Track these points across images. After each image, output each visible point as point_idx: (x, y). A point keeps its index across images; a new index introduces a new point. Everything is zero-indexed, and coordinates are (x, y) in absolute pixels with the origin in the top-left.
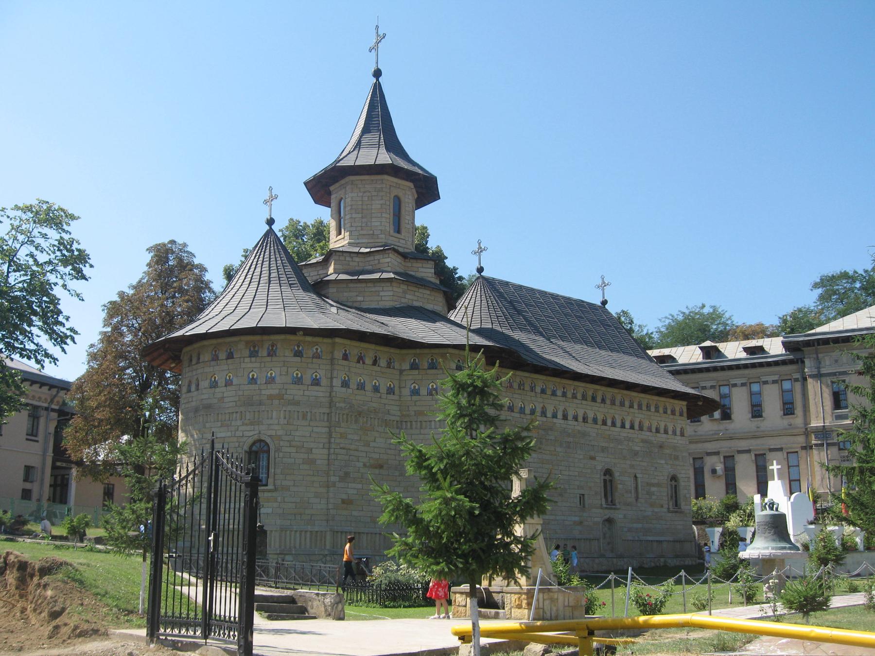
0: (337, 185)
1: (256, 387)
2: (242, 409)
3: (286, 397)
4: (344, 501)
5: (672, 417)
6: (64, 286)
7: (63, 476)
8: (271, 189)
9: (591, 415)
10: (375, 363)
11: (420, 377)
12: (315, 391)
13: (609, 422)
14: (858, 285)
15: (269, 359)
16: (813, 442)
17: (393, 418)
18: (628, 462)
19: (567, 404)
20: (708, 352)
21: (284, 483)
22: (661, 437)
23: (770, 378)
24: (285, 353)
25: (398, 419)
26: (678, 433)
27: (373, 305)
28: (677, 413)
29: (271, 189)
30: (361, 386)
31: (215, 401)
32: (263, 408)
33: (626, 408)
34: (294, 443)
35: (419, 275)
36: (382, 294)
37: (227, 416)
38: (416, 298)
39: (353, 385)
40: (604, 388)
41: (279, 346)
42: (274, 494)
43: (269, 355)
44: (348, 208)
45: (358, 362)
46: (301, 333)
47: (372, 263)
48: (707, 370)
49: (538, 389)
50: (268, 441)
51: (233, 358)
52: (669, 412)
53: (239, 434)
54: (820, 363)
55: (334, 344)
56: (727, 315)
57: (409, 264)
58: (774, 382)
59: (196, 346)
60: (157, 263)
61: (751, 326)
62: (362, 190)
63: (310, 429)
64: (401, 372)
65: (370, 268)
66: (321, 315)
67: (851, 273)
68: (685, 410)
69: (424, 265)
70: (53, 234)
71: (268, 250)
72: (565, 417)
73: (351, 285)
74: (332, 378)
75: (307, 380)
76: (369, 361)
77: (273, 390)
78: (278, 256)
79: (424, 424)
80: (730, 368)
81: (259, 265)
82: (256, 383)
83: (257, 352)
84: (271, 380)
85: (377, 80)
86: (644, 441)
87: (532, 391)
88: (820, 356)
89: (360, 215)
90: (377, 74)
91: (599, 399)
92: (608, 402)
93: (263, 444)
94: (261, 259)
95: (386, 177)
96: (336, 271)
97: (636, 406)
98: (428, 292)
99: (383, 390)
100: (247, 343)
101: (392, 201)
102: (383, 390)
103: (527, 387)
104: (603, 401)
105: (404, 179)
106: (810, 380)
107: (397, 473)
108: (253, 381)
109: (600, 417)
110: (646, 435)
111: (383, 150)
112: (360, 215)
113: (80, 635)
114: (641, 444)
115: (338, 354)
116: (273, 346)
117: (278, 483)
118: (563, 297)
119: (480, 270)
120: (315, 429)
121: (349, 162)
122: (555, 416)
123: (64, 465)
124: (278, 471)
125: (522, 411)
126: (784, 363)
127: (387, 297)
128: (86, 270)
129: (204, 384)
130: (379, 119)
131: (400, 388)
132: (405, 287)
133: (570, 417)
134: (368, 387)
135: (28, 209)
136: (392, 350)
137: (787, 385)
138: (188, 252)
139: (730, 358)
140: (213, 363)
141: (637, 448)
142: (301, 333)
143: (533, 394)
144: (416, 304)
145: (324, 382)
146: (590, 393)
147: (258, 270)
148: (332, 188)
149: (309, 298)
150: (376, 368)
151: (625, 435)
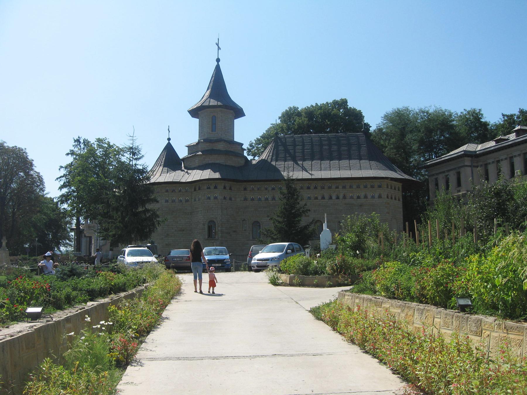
4: (166, 245)
35: (218, 148)
45: (173, 192)
90: (218, 60)
144: (210, 162)
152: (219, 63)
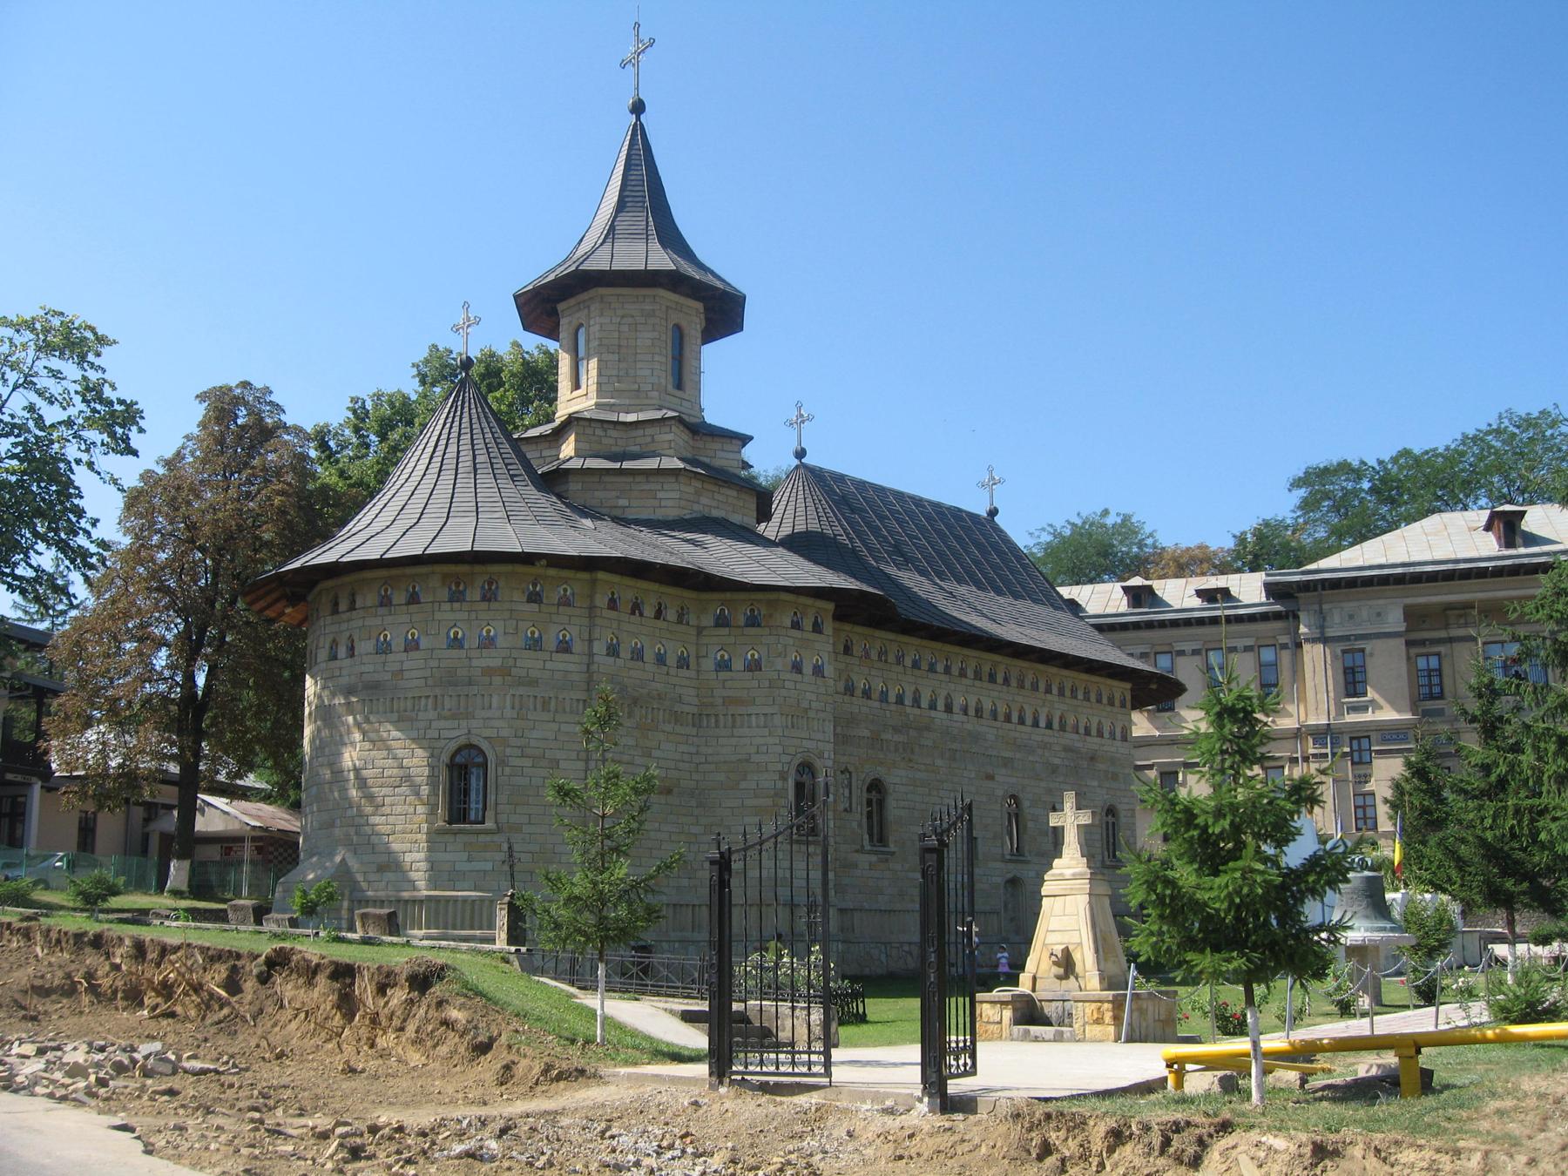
0: (572, 301)
1: (462, 653)
2: (438, 691)
3: (514, 671)
5: (1109, 708)
6: (90, 465)
7: (14, 798)
8: (466, 306)
9: (987, 706)
10: (659, 614)
11: (732, 640)
12: (561, 662)
13: (1015, 718)
14: (1366, 485)
15: (484, 605)
16: (1311, 751)
17: (687, 709)
18: (1043, 784)
19: (952, 686)
20: (1138, 597)
21: (514, 819)
22: (1093, 742)
23: (1240, 643)
24: (513, 595)
25: (695, 710)
26: (1118, 735)
27: (644, 515)
28: (1117, 703)
29: (466, 306)
30: (638, 655)
31: (388, 676)
32: (475, 689)
33: (1041, 694)
34: (528, 751)
35: (717, 463)
36: (660, 495)
37: (409, 704)
38: (714, 504)
39: (625, 653)
40: (1008, 660)
41: (502, 583)
42: (496, 838)
43: (484, 598)
44: (594, 344)
45: (633, 613)
46: (544, 562)
47: (638, 440)
48: (1136, 626)
49: (908, 662)
50: (484, 746)
51: (419, 603)
52: (1105, 700)
53: (433, 734)
54: (1324, 619)
55: (594, 582)
56: (1147, 529)
57: (700, 444)
58: (1248, 649)
59: (347, 579)
60: (219, 420)
61: (1188, 549)
62: (620, 312)
63: (555, 726)
64: (700, 630)
65: (636, 449)
66: (572, 531)
67: (1355, 464)
68: (1128, 697)
69: (727, 447)
70: (71, 370)
71: (466, 415)
72: (949, 708)
73: (607, 479)
74: (590, 641)
75: (550, 642)
76: (649, 611)
77: (492, 660)
78: (485, 425)
79: (738, 719)
80: (1175, 623)
81: (453, 441)
82: (461, 647)
83: (462, 593)
84: (488, 643)
85: (638, 118)
86: (1067, 749)
87: (898, 663)
88: (1325, 607)
89: (616, 357)
90: (638, 108)
91: (1000, 679)
92: (1014, 683)
93: (474, 753)
94: (456, 429)
95: (662, 292)
96: (579, 453)
97: (1055, 690)
98: (735, 493)
99: (672, 660)
100: (445, 576)
101: (670, 333)
102: (672, 660)
103: (891, 658)
104: (1006, 681)
105: (688, 296)
106: (1306, 647)
107: (693, 803)
108: (456, 643)
109: (1002, 709)
110: (1069, 738)
111: (655, 245)
112: (616, 357)
113: (559, 1078)
114: (1063, 754)
115: (601, 600)
116: (490, 584)
117: (503, 818)
118: (930, 502)
119: (801, 454)
120: (564, 727)
121: (600, 263)
122: (933, 706)
123: (19, 778)
124: (503, 798)
125: (884, 697)
126: (1264, 617)
127: (671, 501)
128: (136, 440)
129: (365, 647)
130: (644, 190)
131: (698, 657)
132: (698, 484)
133: (956, 709)
134: (649, 655)
135: (29, 325)
136: (687, 594)
137: (1268, 655)
138: (271, 403)
139: (1177, 607)
140: (381, 611)
141: (1057, 761)
142: (544, 562)
143: (900, 668)
144: (715, 513)
145: (578, 647)
146: (986, 669)
147: (453, 448)
148: (561, 307)
149: (545, 502)
150: (660, 623)
151: (1039, 738)
152: (642, 117)
